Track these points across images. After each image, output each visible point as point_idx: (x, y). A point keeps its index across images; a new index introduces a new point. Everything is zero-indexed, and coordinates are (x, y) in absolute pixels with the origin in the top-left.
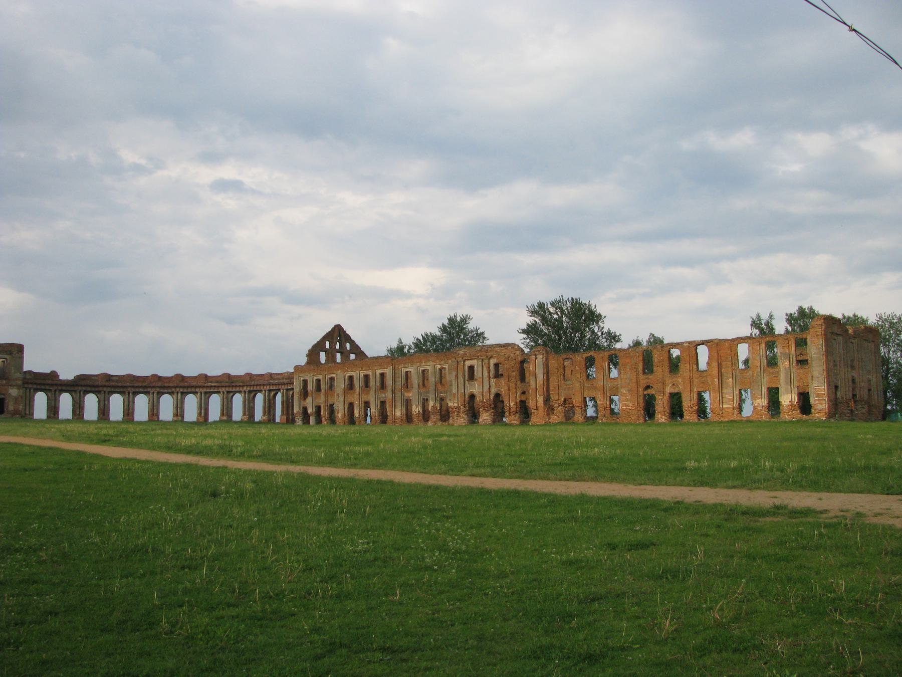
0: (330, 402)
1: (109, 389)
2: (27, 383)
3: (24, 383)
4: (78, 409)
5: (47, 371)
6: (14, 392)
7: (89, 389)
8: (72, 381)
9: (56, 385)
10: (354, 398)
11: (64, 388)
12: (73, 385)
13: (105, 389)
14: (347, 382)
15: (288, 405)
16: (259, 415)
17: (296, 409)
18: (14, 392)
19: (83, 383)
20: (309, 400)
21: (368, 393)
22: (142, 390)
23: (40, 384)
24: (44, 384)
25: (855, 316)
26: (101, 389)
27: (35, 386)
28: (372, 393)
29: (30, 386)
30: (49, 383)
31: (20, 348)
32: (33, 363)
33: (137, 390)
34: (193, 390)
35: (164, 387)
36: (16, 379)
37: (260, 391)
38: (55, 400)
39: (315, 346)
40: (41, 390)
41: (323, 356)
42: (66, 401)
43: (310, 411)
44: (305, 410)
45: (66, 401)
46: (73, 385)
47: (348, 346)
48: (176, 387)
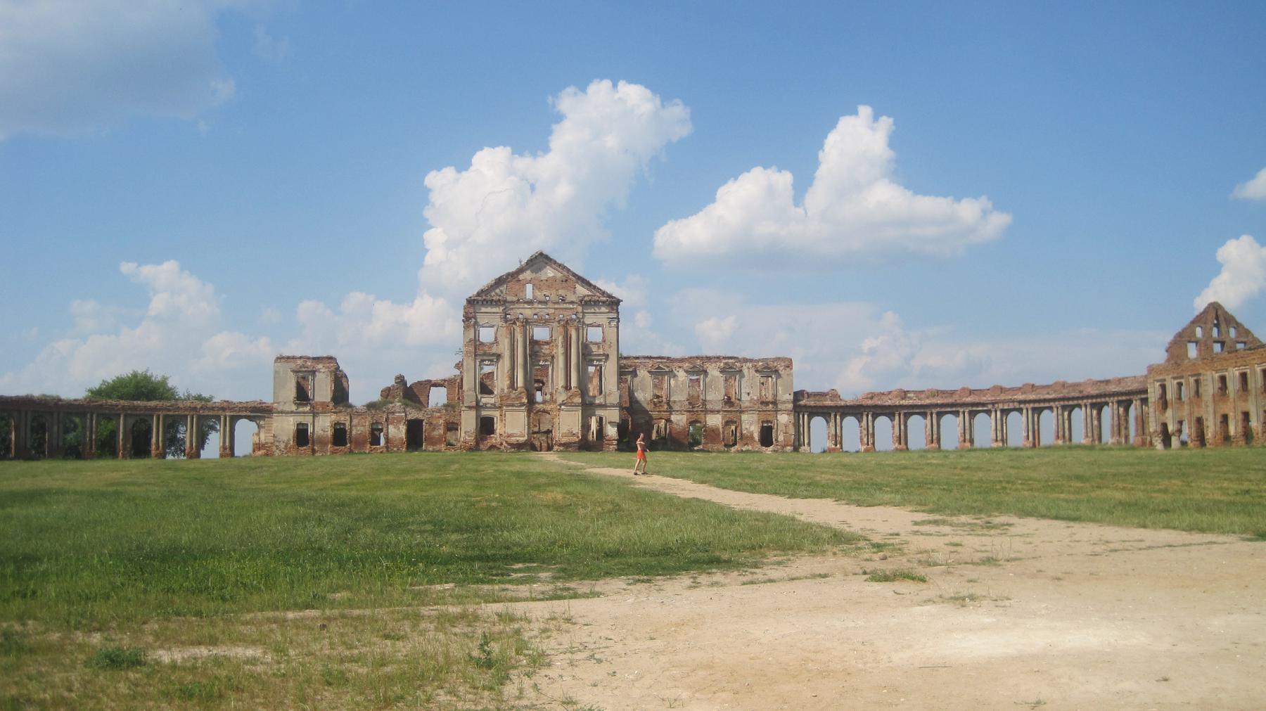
0: (1197, 415)
10: (1228, 408)
14: (1218, 385)
15: (1142, 422)
16: (1108, 438)
17: (1153, 427)
19: (870, 402)
20: (1169, 412)
21: (1246, 401)
25: (427, 251)
28: (1251, 399)
31: (789, 364)
32: (806, 379)
34: (1017, 405)
35: (977, 404)
36: (784, 402)
37: (1079, 406)
39: (1180, 335)
40: (818, 414)
41: (1192, 352)
43: (1170, 428)
44: (1165, 425)
47: (1232, 333)
48: (993, 404)
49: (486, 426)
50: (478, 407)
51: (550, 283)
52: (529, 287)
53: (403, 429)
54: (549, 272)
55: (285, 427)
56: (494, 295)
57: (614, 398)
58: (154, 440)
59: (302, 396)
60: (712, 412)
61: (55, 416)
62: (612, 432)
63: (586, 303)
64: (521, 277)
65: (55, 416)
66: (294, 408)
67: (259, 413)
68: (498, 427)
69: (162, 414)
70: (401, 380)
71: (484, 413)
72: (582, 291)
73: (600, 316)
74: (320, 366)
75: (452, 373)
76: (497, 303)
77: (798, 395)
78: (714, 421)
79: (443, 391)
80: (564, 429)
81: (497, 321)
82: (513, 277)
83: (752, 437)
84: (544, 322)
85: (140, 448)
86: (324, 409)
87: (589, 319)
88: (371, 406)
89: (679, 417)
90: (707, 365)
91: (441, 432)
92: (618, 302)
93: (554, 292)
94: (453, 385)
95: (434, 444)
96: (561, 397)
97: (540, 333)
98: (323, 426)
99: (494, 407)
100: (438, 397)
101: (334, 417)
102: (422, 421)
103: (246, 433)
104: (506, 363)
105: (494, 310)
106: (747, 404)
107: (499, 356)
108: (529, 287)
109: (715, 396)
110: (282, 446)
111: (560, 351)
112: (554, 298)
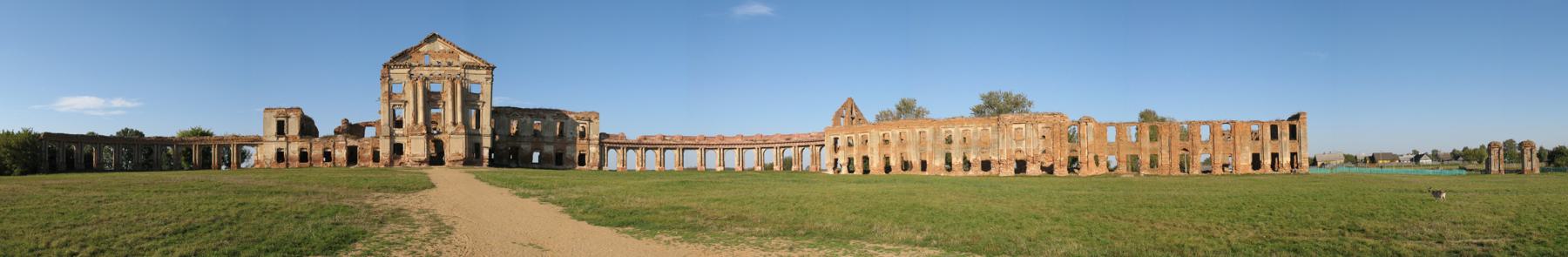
51: (441, 54)
54: (439, 46)
55: (268, 152)
59: (281, 129)
62: (486, 153)
63: (467, 66)
67: (256, 141)
68: (406, 150)
71: (398, 140)
72: (464, 58)
73: (478, 76)
77: (603, 136)
78: (549, 149)
81: (405, 78)
82: (416, 49)
85: (206, 164)
86: (294, 139)
96: (450, 129)
97: (434, 88)
98: (294, 150)
100: (370, 132)
104: (410, 107)
111: (448, 98)
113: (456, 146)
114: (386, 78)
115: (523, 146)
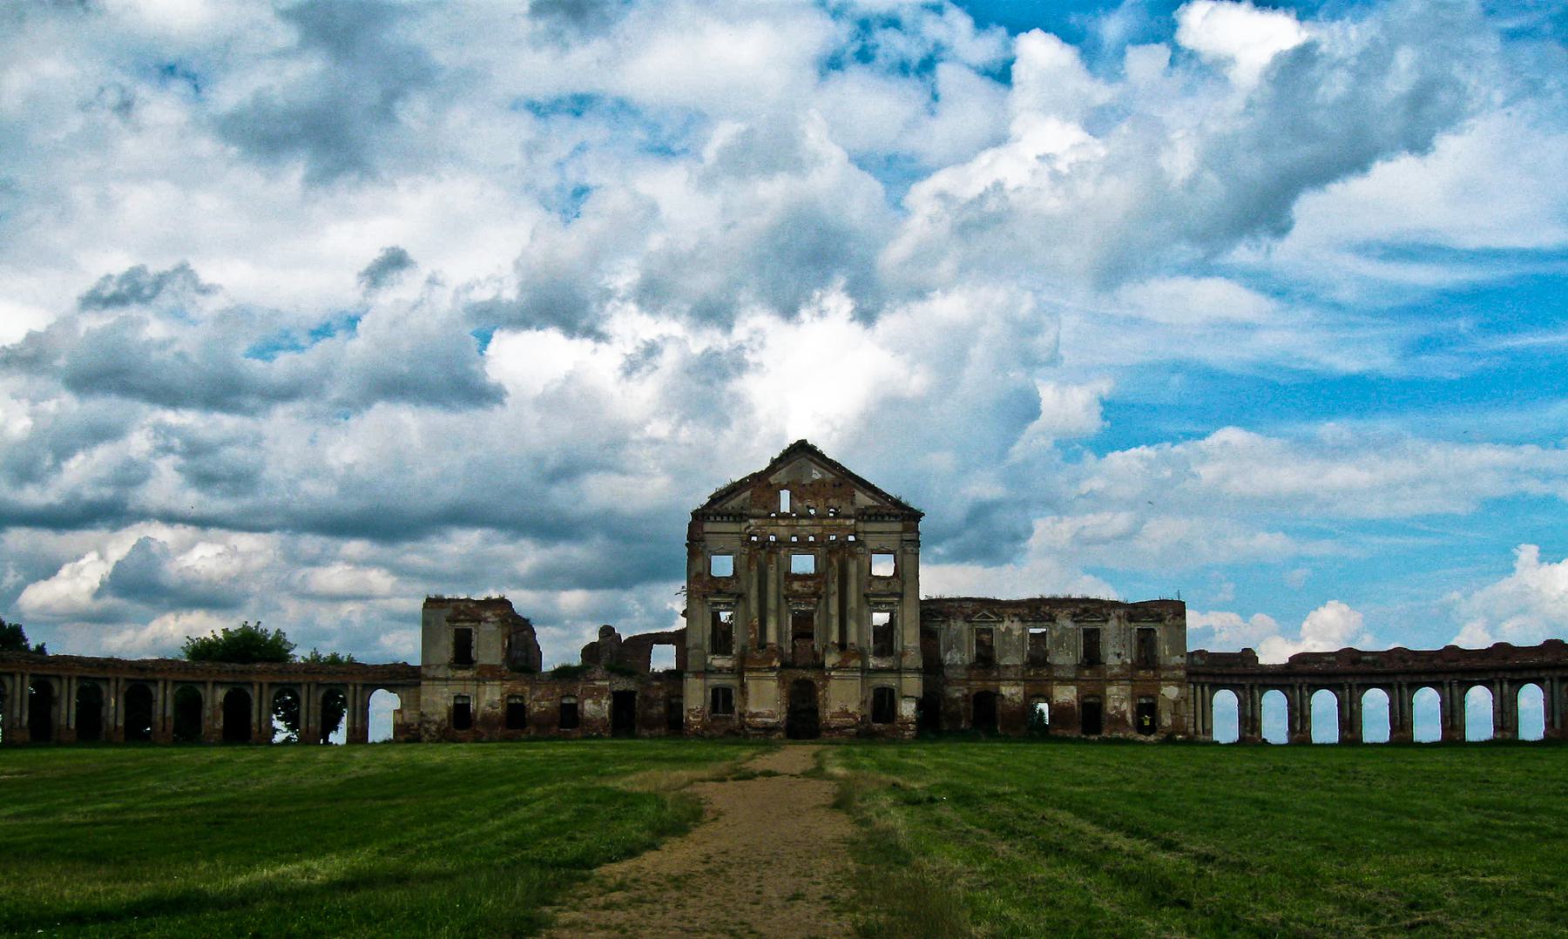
1: (1358, 681)
2: (1196, 674)
3: (1189, 674)
4: (1299, 718)
5: (1236, 649)
6: (1171, 692)
7: (1318, 681)
8: (1286, 666)
9: (1252, 675)
11: (1268, 681)
12: (1287, 675)
13: (1350, 680)
18: (1171, 692)
19: (1306, 668)
22: (1424, 678)
23: (1222, 675)
24: (1230, 675)
26: (1341, 680)
27: (1211, 680)
29: (1203, 679)
30: (1241, 672)
31: (1177, 609)
33: (1416, 679)
34: (1534, 675)
36: (1173, 668)
38: (1253, 703)
40: (1225, 687)
42: (1274, 706)
45: (1274, 706)
46: (1287, 675)
49: (721, 700)
50: (706, 672)
51: (816, 490)
52: (785, 496)
53: (606, 704)
55: (438, 700)
56: (733, 504)
57: (914, 659)
58: (255, 719)
59: (463, 654)
60: (1064, 682)
61: (113, 684)
62: (907, 709)
64: (772, 480)
65: (113, 684)
66: (450, 673)
67: (398, 677)
68: (736, 701)
69: (265, 680)
70: (607, 632)
72: (863, 499)
74: (488, 614)
75: (681, 623)
76: (739, 516)
78: (1066, 695)
79: (671, 649)
80: (835, 707)
83: (1123, 719)
84: (804, 547)
87: (872, 542)
88: (564, 673)
89: (1014, 690)
90: (1056, 612)
91: (662, 709)
92: (916, 516)
93: (821, 501)
94: (678, 638)
95: (650, 727)
97: (803, 564)
98: (489, 698)
99: (731, 670)
100: (663, 659)
101: (508, 685)
102: (633, 693)
103: (384, 708)
105: (733, 527)
106: (1116, 670)
107: (740, 597)
108: (785, 496)
109: (1065, 658)
110: (434, 728)
111: (834, 587)
112: (821, 509)
113: (843, 697)
114: (697, 543)
115: (1006, 690)
